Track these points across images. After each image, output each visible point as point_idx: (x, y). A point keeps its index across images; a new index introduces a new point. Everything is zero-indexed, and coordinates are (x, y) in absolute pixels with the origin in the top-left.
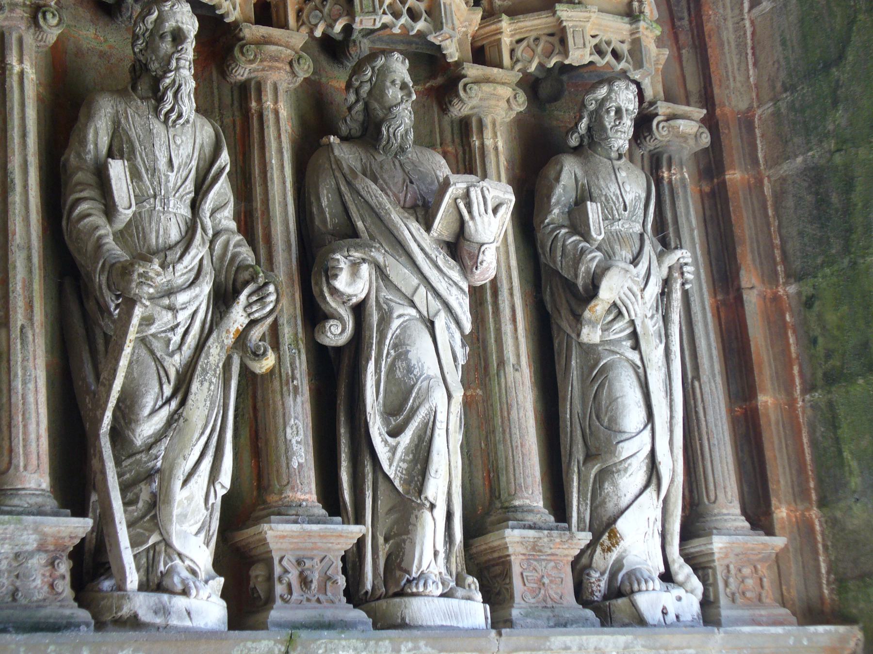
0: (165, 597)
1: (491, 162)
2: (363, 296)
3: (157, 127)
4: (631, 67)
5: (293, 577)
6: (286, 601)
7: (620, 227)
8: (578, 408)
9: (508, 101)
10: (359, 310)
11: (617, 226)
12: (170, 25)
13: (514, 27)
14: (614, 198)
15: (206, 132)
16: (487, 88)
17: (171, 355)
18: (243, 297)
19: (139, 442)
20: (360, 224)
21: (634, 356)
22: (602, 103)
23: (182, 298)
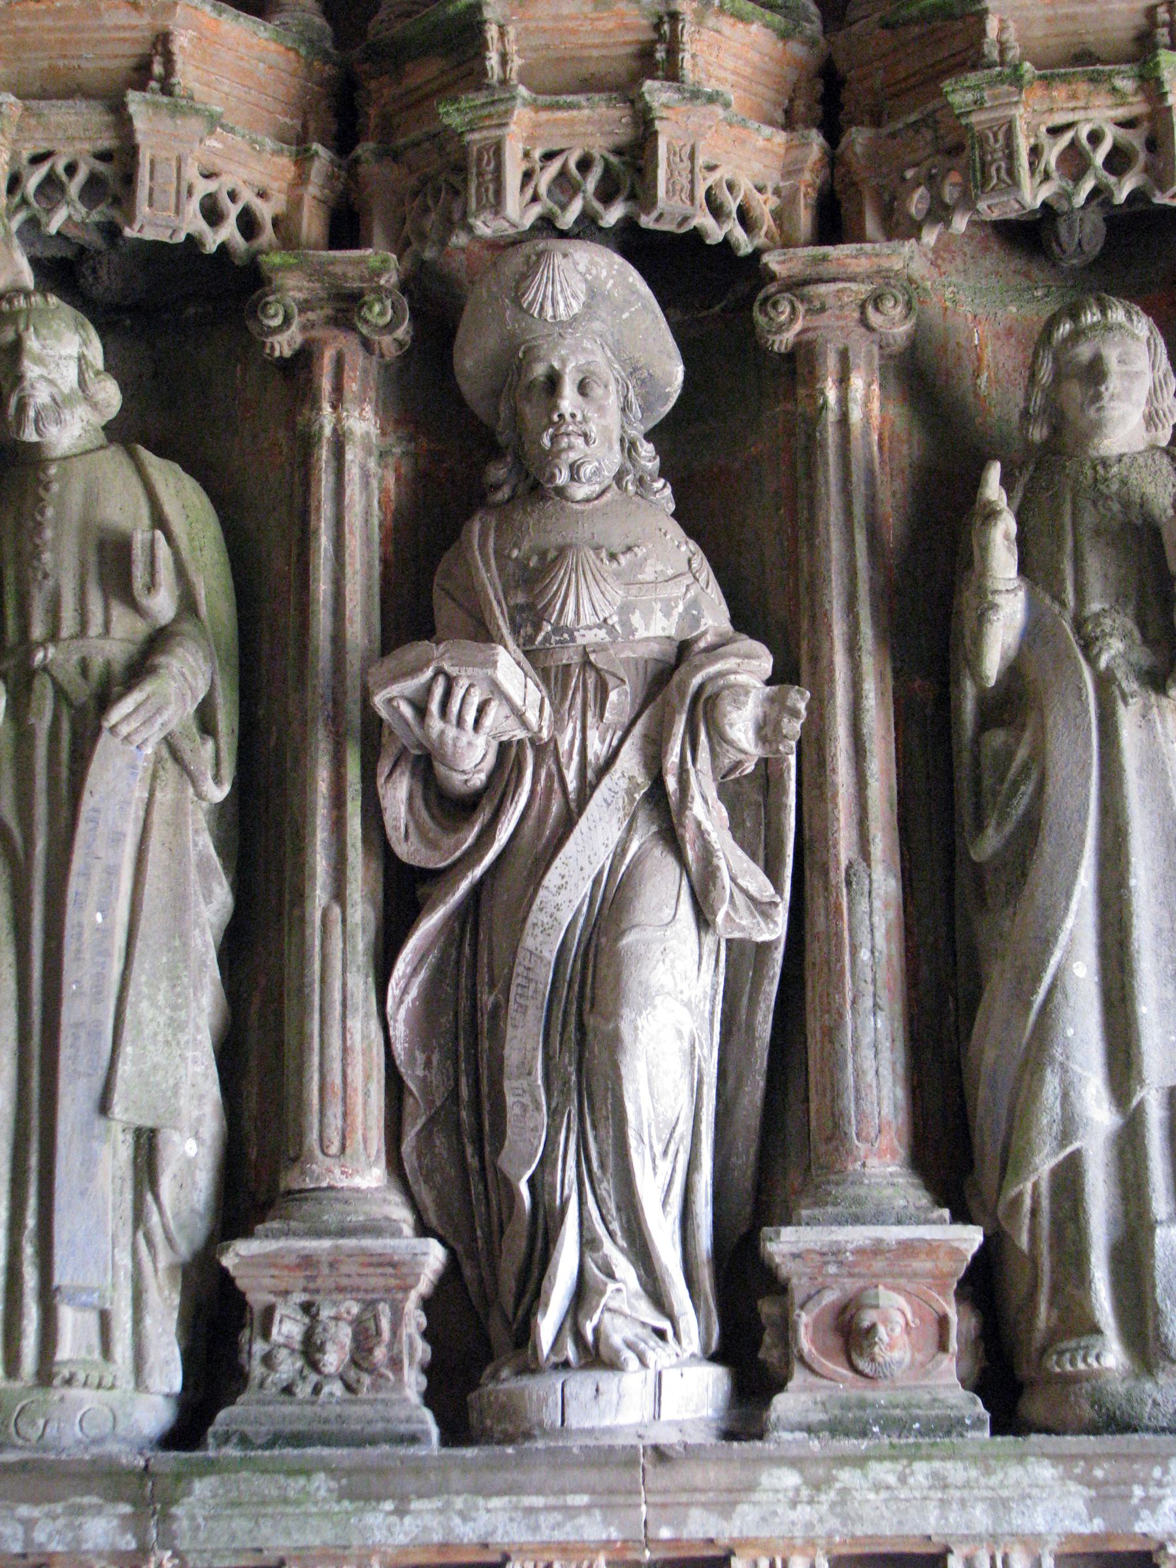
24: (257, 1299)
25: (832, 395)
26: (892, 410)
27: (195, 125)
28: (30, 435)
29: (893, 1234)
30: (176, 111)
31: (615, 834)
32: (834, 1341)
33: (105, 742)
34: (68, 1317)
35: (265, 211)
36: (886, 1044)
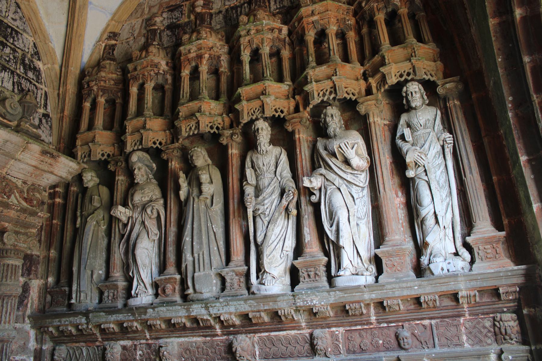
0: (260, 286)
2: (319, 186)
3: (259, 156)
4: (414, 76)
5: (305, 274)
6: (303, 282)
10: (320, 189)
11: (419, 133)
12: (256, 128)
13: (375, 79)
15: (276, 150)
16: (366, 104)
17: (265, 218)
18: (284, 196)
19: (259, 244)
20: (321, 163)
21: (426, 178)
22: (406, 92)
23: (266, 202)
24: (103, 290)
25: (170, 164)
26: (182, 165)
27: (97, 145)
28: (85, 186)
29: (167, 277)
30: (95, 144)
31: (139, 227)
32: (163, 292)
33: (88, 223)
34: (82, 294)
35: (111, 154)
36: (172, 251)
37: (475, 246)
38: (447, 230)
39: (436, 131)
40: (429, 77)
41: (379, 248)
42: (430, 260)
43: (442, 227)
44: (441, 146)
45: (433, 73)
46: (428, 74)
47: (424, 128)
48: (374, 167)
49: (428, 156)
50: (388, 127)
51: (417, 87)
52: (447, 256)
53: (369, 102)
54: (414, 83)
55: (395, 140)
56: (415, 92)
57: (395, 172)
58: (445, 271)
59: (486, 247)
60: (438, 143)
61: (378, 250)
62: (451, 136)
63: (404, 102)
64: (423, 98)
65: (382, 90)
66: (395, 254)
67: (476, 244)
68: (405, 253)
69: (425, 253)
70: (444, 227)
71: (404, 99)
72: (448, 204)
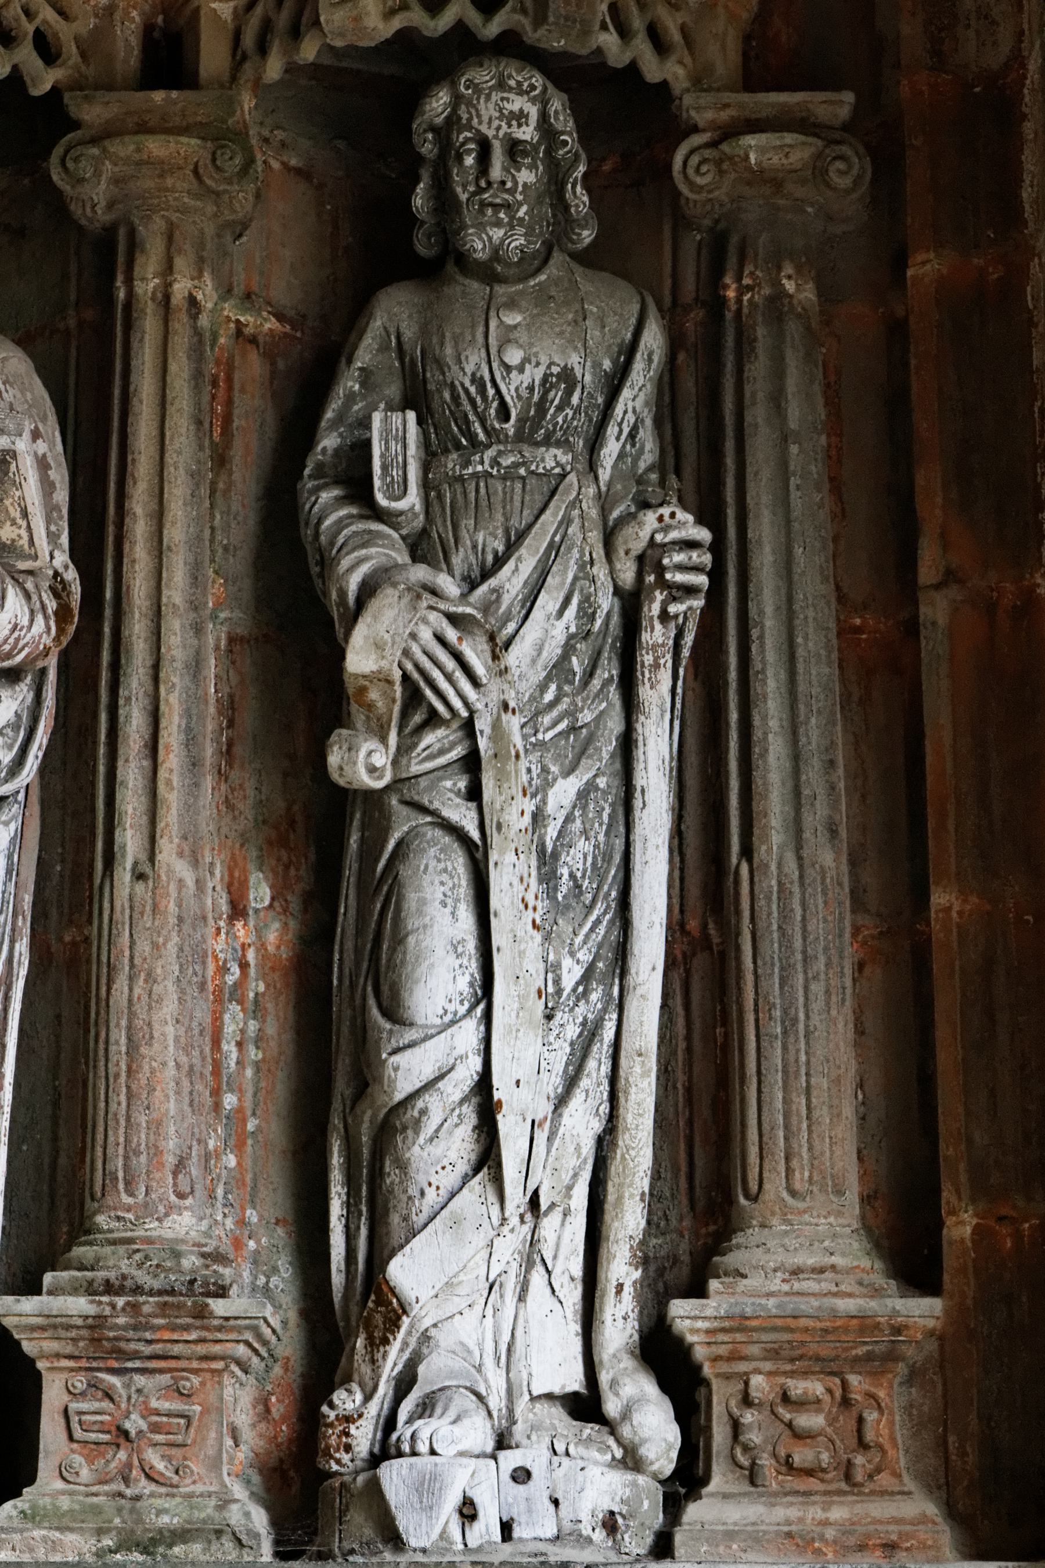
1: (141, 340)
4: (526, 22)
7: (487, 466)
8: (349, 956)
9: (196, 172)
14: (473, 390)
16: (123, 148)
22: (444, 132)
37: (724, 1368)
38: (549, 1225)
39: (605, 474)
40: (642, 48)
41: (34, 1288)
42: (390, 1424)
43: (516, 1197)
44: (617, 591)
45: (671, 25)
46: (637, 23)
47: (520, 437)
48: (106, 657)
49: (514, 657)
50: (269, 356)
51: (533, 112)
52: (522, 1404)
53: (156, 147)
54: (518, 75)
55: (300, 476)
56: (514, 149)
57: (248, 719)
58: (487, 1527)
59: (798, 1387)
60: (600, 571)
61: (29, 1304)
62: (704, 535)
63: (420, 200)
64: (561, 204)
65: (274, 69)
66: (147, 1350)
67: (734, 1357)
68: (217, 1349)
69: (366, 1369)
70: (535, 1195)
71: (426, 175)
72: (590, 1034)
